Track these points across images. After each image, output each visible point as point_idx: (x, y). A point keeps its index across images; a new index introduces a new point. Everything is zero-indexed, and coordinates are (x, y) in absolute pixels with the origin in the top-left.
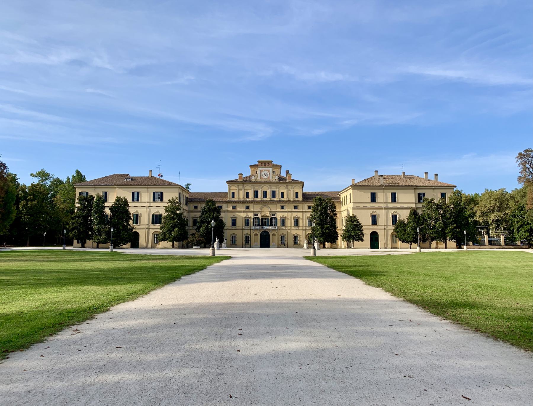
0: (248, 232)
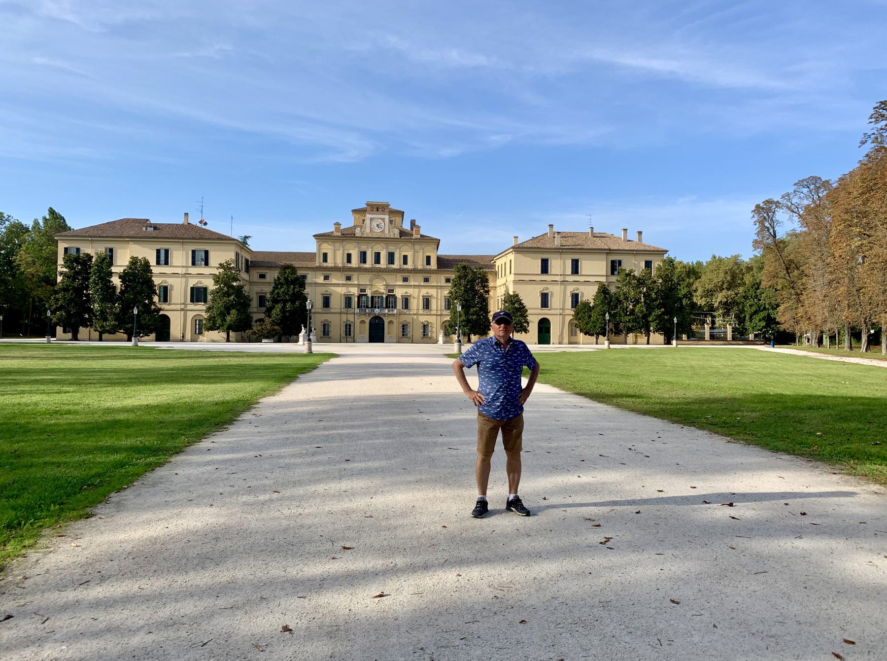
0: (351, 318)
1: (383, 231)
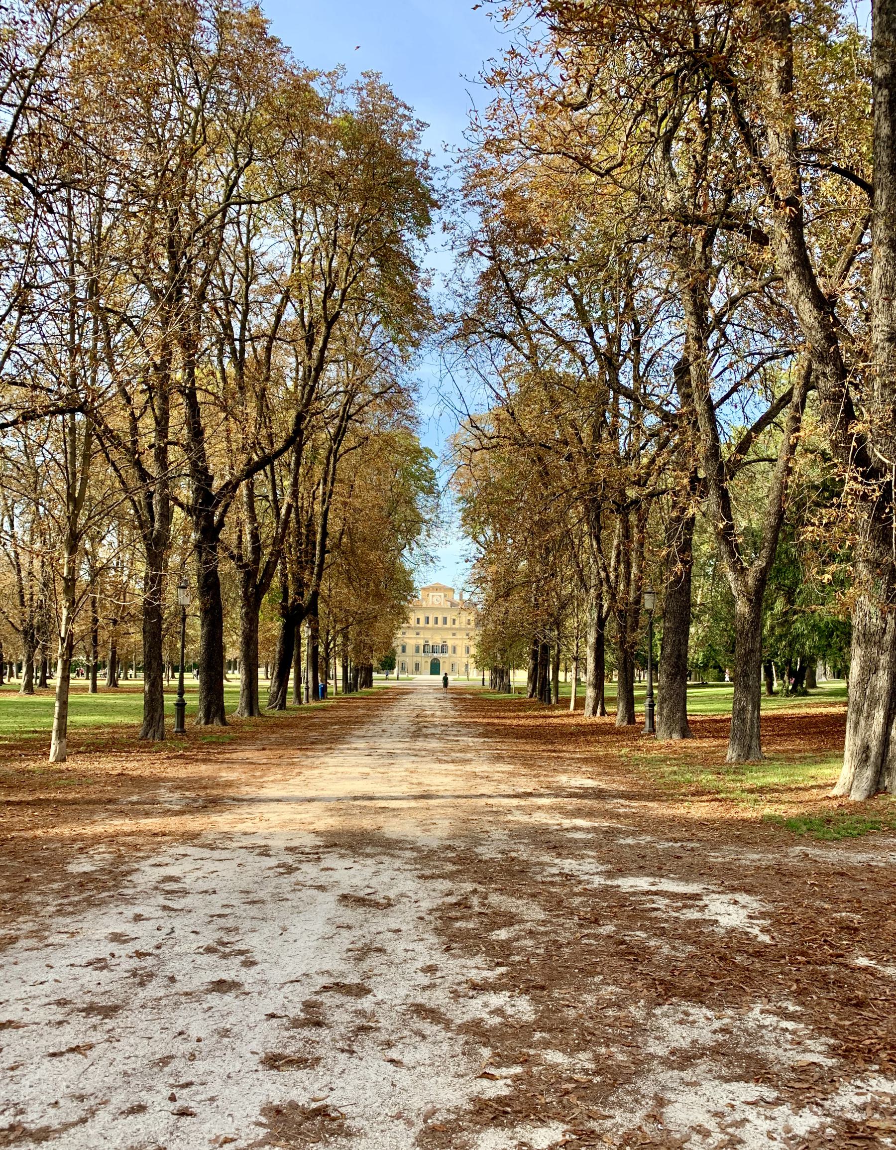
0: (419, 659)
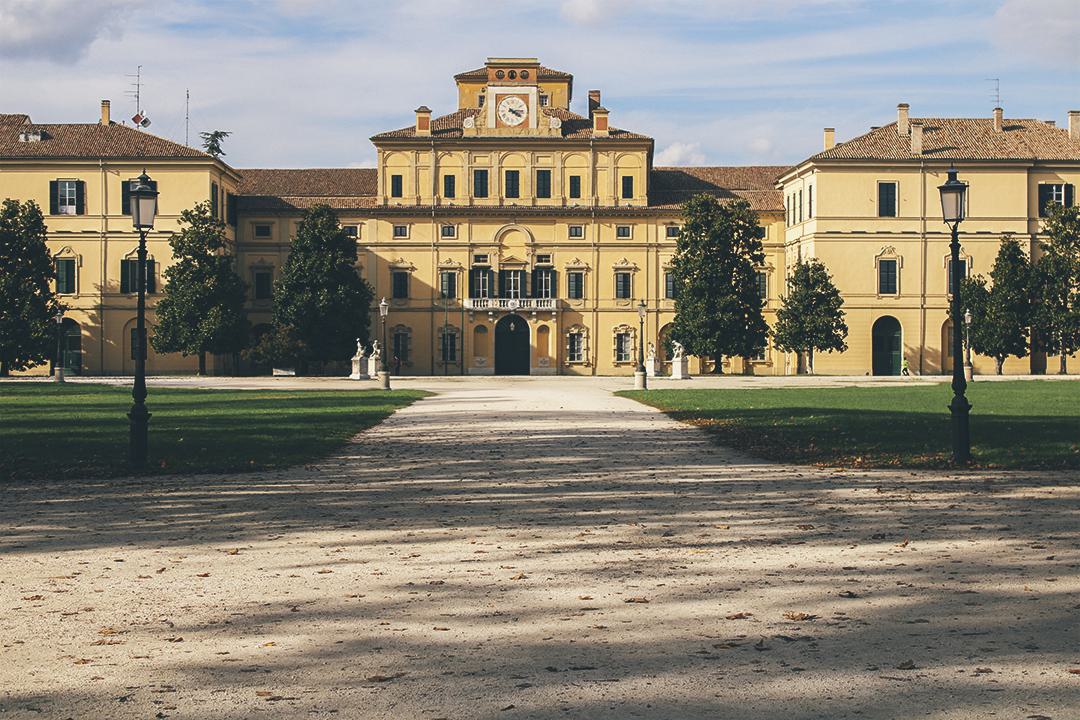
1: (525, 124)
